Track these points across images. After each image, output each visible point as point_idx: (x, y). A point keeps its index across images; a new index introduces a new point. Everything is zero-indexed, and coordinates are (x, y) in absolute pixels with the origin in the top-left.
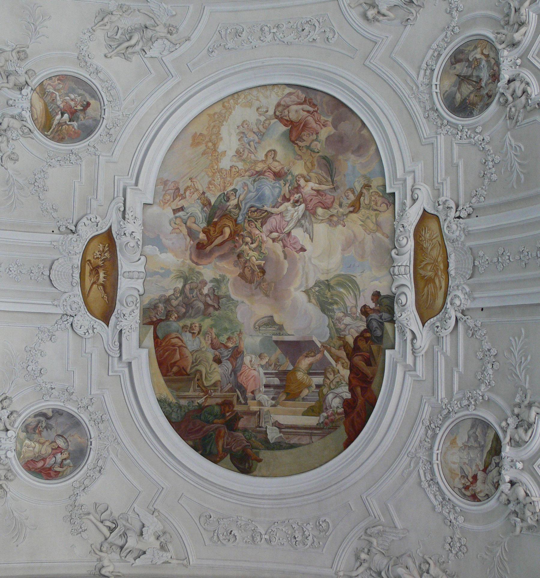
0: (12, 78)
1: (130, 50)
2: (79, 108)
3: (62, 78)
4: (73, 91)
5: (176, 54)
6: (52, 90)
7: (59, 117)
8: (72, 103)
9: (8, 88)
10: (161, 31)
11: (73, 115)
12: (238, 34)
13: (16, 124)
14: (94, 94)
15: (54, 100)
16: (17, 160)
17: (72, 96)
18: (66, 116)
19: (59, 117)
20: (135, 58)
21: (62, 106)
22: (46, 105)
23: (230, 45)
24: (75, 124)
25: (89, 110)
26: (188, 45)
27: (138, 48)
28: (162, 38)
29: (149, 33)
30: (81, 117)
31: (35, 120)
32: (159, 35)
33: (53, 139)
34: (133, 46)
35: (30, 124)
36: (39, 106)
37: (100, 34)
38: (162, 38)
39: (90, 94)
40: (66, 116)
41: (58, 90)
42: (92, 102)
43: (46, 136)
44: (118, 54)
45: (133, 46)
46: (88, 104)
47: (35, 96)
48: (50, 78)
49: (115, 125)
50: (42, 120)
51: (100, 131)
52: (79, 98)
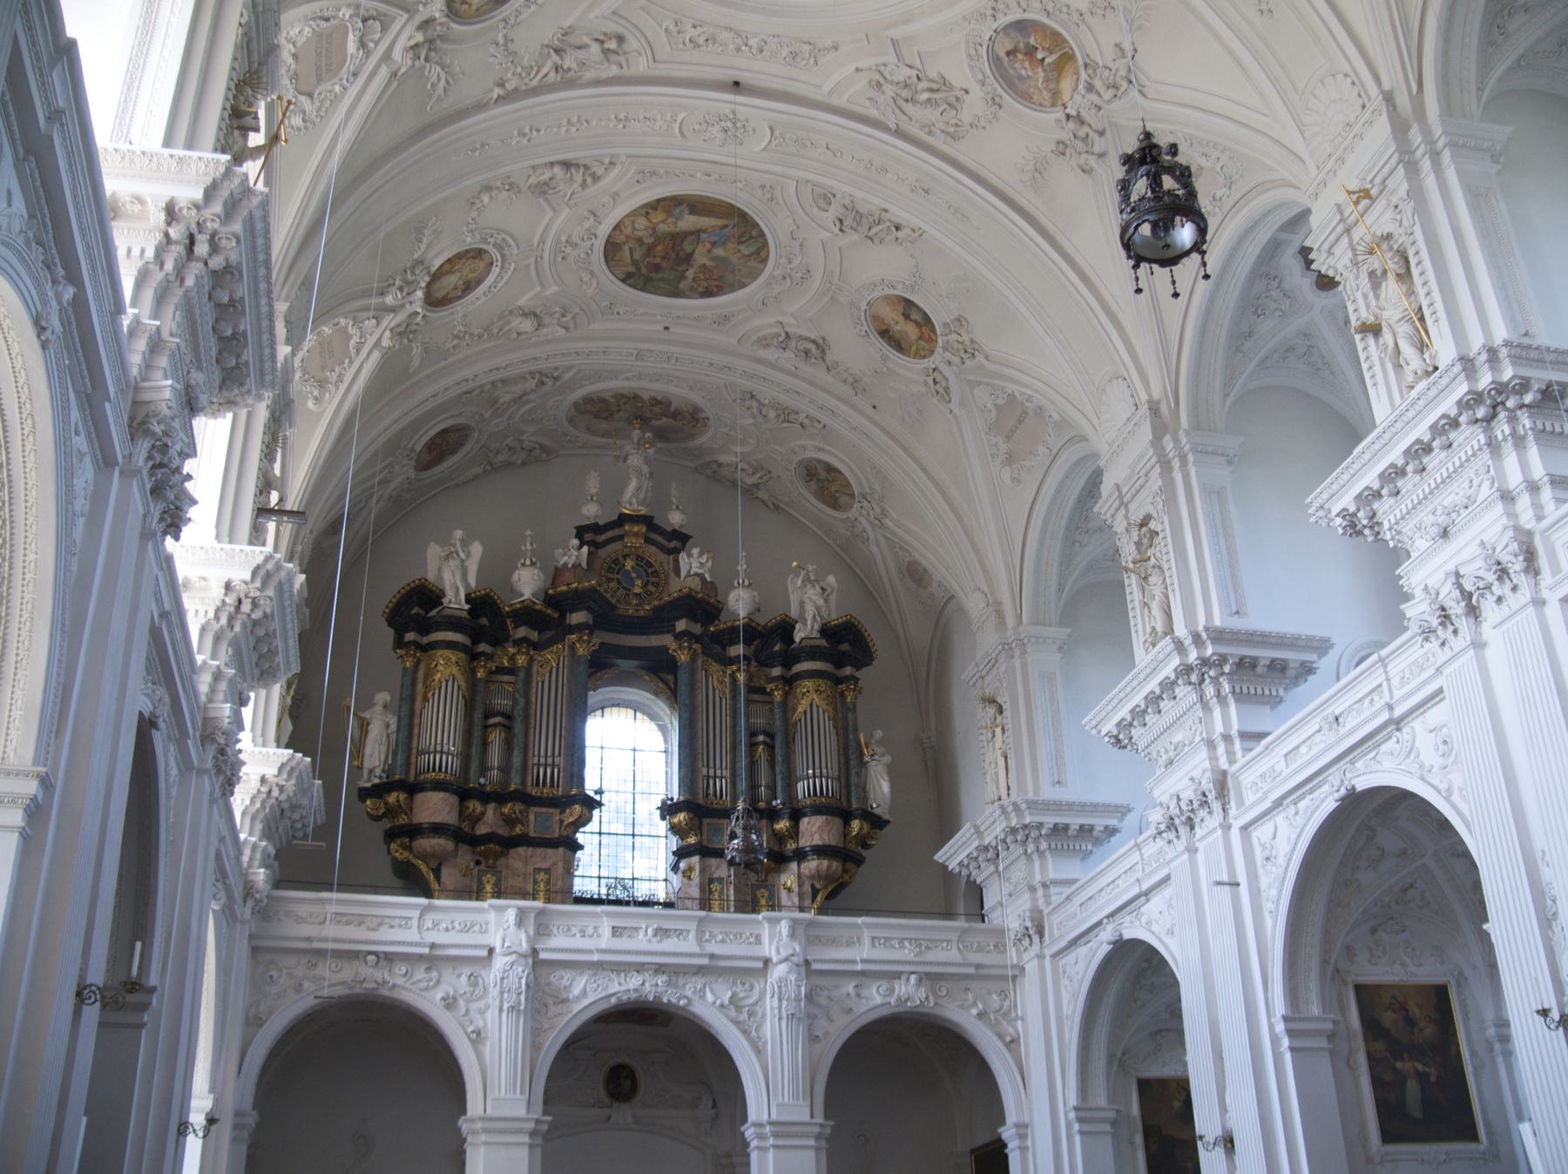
0: (1081, 133)
1: (935, 86)
2: (1020, 56)
3: (1026, 97)
4: (1021, 78)
5: (881, 60)
6: (1045, 92)
7: (1048, 60)
8: (1026, 64)
9: (1090, 126)
10: (888, 88)
11: (1030, 52)
12: (794, 55)
13: (1098, 84)
14: (995, 61)
15: (1046, 80)
16: (1117, 45)
17: (1023, 72)
18: (1040, 55)
19: (1048, 60)
20: (933, 74)
21: (1040, 69)
22: (1058, 81)
23: (807, 48)
24: (1032, 41)
25: (1009, 46)
26: (861, 65)
27: (924, 84)
28: (892, 83)
29: (905, 93)
30: (1021, 45)
31: (1077, 73)
32: (895, 88)
33: (1065, 41)
34: (931, 90)
35: (1083, 76)
36: (1066, 85)
37: (966, 117)
38: (892, 83)
39: (1002, 64)
40: (1040, 55)
41: (1037, 87)
42: (1002, 54)
43: (1071, 48)
44: (951, 88)
45: (931, 90)
46: (1008, 53)
47: (1066, 98)
48: (1041, 105)
49: (983, 16)
50: (1069, 69)
51: (1003, 20)
52: (1017, 66)
